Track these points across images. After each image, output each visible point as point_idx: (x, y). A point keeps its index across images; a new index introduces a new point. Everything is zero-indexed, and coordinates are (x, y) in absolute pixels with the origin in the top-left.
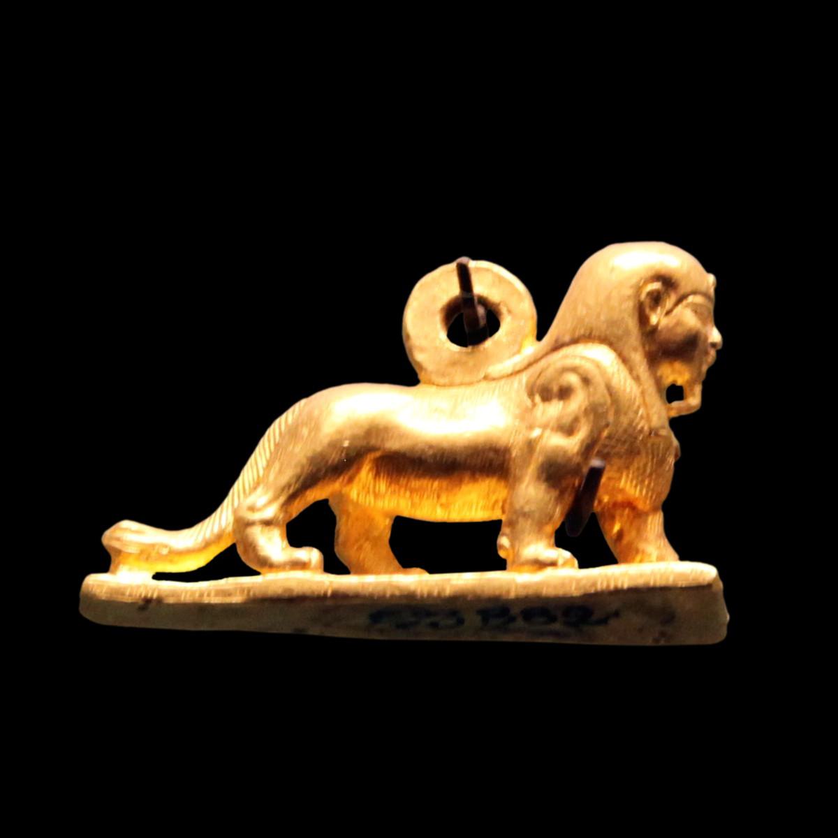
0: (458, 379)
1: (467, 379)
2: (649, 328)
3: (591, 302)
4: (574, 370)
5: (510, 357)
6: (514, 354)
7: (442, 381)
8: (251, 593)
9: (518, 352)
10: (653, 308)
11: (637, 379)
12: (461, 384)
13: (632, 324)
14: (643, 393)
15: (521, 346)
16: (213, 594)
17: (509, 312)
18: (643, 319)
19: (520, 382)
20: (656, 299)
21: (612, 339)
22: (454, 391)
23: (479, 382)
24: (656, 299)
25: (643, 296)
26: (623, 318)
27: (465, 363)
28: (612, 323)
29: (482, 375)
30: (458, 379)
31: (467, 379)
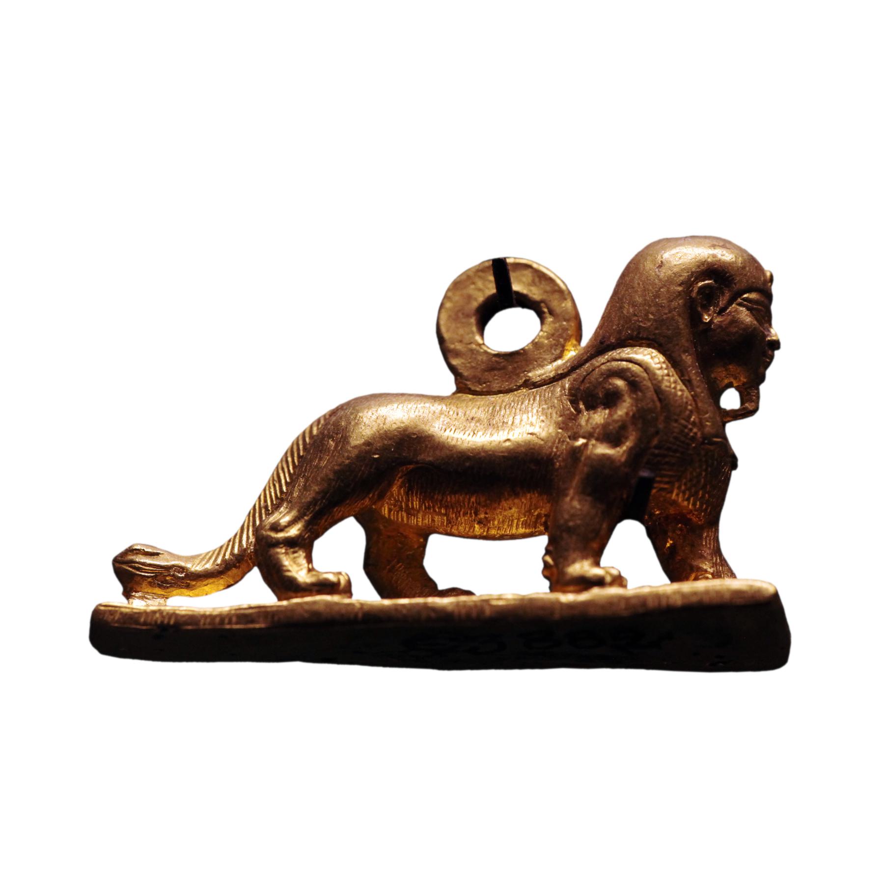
0: (496, 386)
1: (506, 385)
2: (701, 327)
3: (639, 299)
4: (621, 373)
5: (551, 363)
6: (555, 359)
7: (478, 388)
8: (276, 618)
9: (560, 357)
10: (706, 308)
11: (687, 383)
12: (500, 392)
13: (682, 323)
14: (695, 397)
15: (562, 352)
16: (234, 619)
17: (551, 312)
18: (694, 318)
19: (563, 388)
20: (708, 297)
21: (662, 340)
22: (492, 398)
23: (518, 388)
24: (708, 297)
25: (694, 295)
26: (673, 319)
27: (504, 368)
28: (661, 322)
29: (521, 382)
30: (496, 386)
31: (506, 385)
